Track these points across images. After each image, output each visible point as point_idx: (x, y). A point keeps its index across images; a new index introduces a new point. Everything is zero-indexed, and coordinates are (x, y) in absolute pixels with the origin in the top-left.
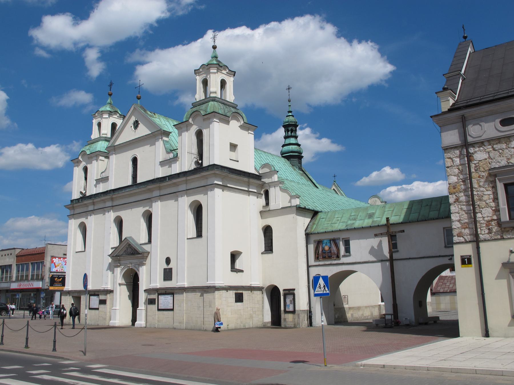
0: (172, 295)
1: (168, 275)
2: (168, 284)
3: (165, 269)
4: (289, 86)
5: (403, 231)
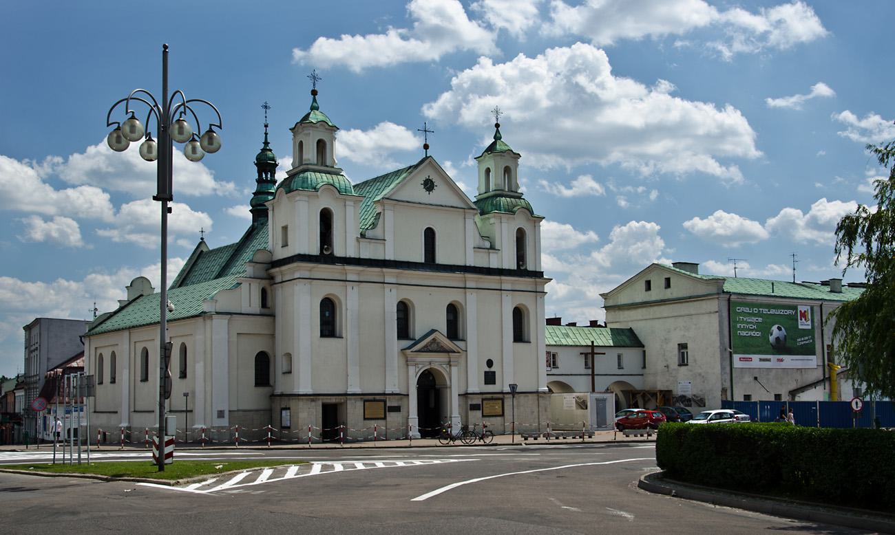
0: (500, 401)
1: (490, 378)
2: (490, 388)
3: (485, 372)
4: (266, 103)
5: (604, 354)
